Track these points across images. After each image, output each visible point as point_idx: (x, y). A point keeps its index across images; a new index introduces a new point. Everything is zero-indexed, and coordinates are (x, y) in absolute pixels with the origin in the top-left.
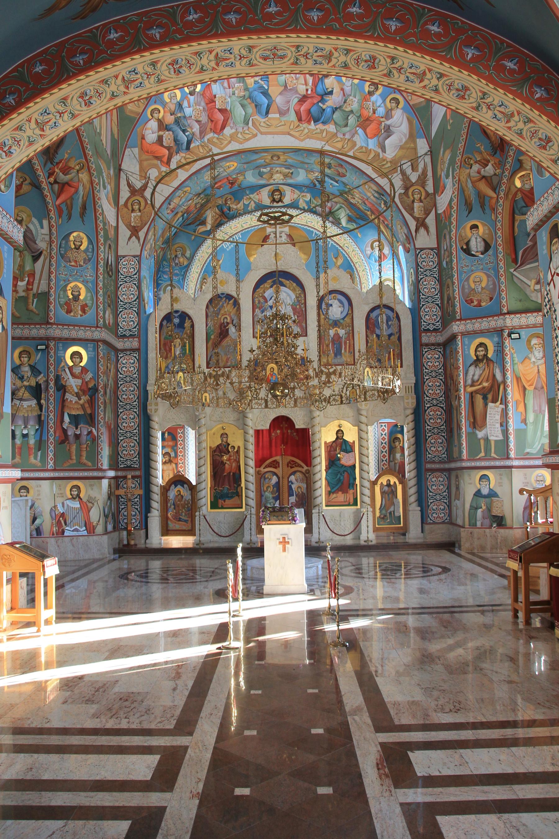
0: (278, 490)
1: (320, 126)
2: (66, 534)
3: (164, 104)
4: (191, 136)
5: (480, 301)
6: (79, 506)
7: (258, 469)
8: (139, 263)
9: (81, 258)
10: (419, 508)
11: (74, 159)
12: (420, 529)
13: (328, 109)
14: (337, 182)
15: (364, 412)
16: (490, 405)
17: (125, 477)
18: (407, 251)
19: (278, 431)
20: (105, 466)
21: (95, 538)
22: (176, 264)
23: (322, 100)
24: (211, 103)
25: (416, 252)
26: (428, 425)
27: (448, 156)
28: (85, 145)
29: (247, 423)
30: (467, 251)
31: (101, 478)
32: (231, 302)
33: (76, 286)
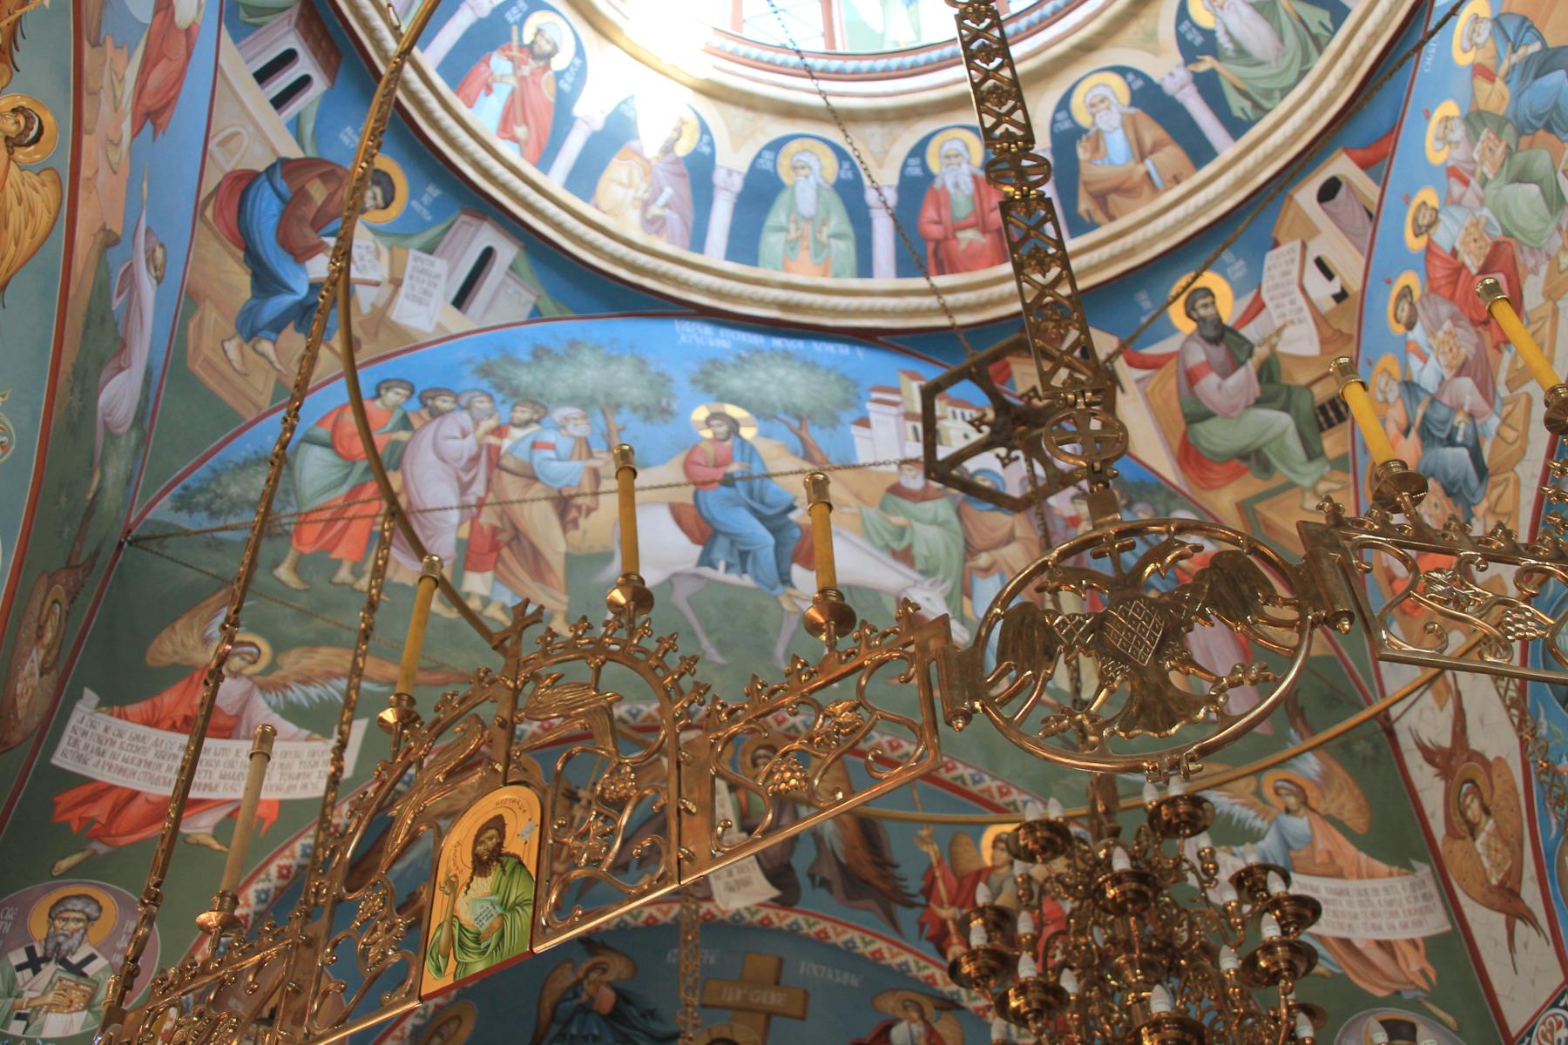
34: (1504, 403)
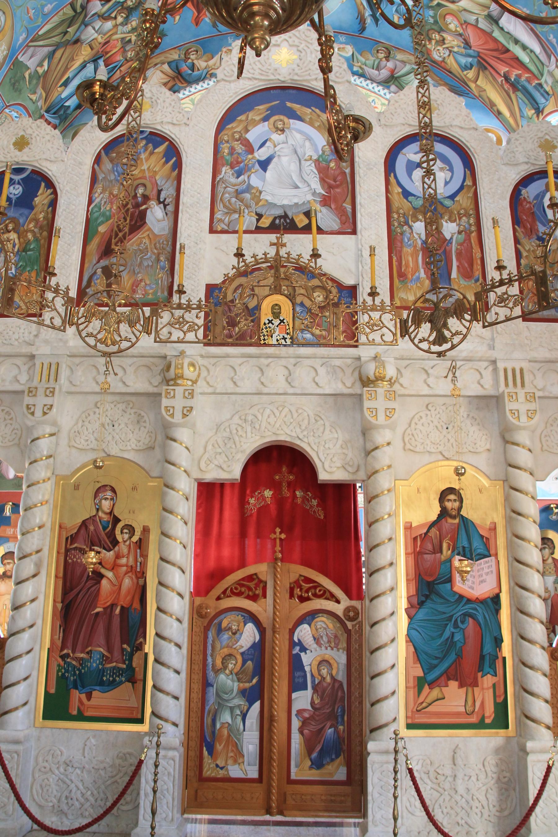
7: (198, 600)
15: (523, 437)
19: (268, 493)
29: (173, 458)
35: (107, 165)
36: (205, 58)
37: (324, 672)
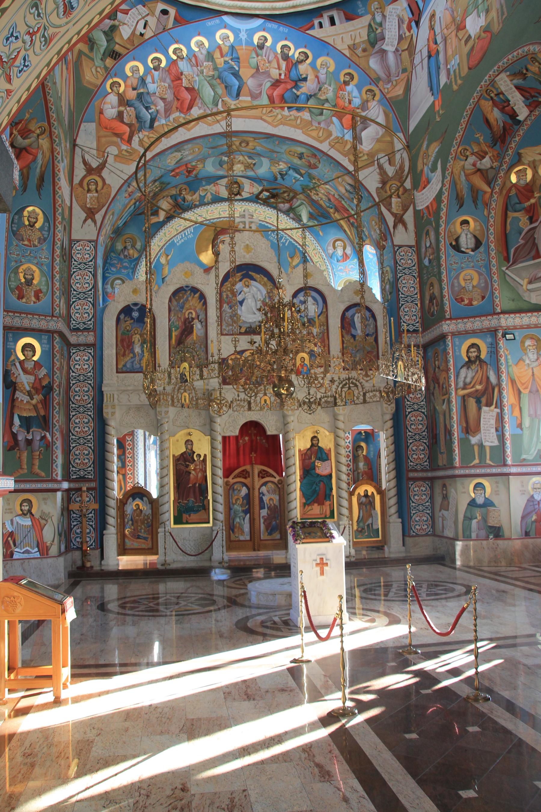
0: (249, 503)
1: (294, 113)
2: (15, 556)
3: (125, 78)
4: (155, 114)
5: (471, 300)
6: (30, 523)
7: (226, 480)
8: (96, 248)
9: (35, 236)
10: (400, 520)
11: (35, 121)
12: (401, 542)
13: (303, 96)
14: (301, 175)
15: (341, 418)
16: (484, 409)
17: (80, 489)
18: (380, 248)
19: (247, 438)
20: (59, 478)
21: (50, 560)
22: (126, 256)
23: (296, 86)
24: (177, 80)
25: (394, 249)
26: (410, 431)
27: (435, 148)
28: (50, 105)
29: (216, 429)
30: (457, 248)
31: (55, 491)
32: (197, 295)
33: (29, 269)
34: (169, 121)
35: (175, 303)
36: (190, 194)
37: (271, 502)
